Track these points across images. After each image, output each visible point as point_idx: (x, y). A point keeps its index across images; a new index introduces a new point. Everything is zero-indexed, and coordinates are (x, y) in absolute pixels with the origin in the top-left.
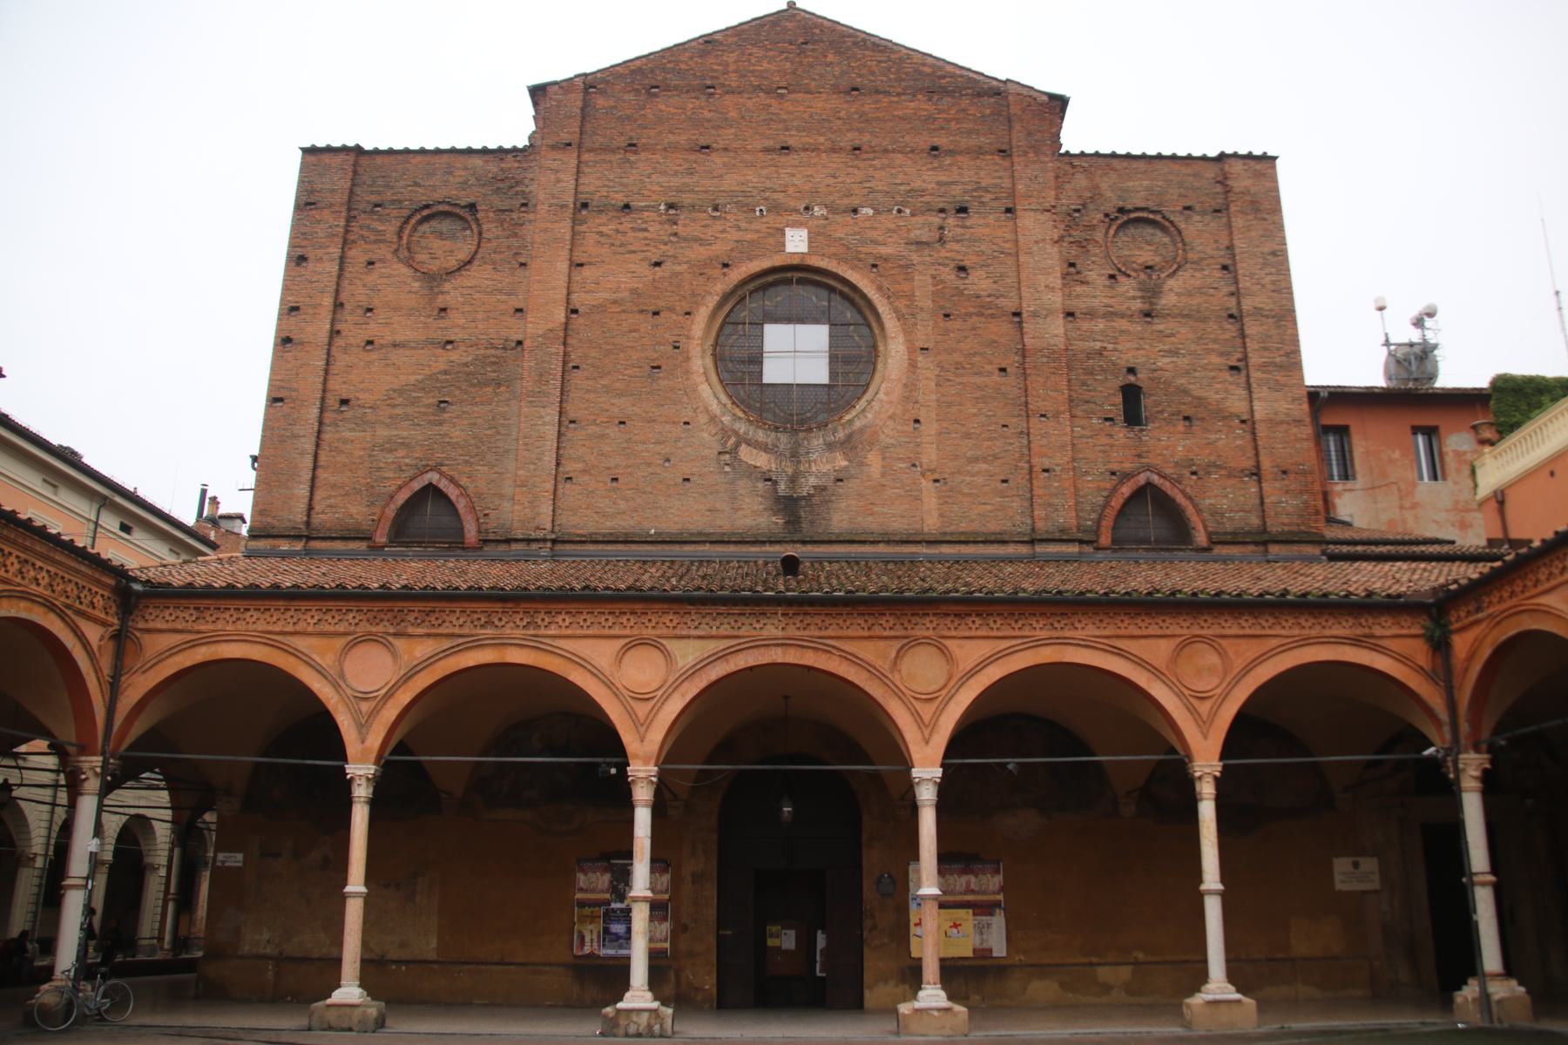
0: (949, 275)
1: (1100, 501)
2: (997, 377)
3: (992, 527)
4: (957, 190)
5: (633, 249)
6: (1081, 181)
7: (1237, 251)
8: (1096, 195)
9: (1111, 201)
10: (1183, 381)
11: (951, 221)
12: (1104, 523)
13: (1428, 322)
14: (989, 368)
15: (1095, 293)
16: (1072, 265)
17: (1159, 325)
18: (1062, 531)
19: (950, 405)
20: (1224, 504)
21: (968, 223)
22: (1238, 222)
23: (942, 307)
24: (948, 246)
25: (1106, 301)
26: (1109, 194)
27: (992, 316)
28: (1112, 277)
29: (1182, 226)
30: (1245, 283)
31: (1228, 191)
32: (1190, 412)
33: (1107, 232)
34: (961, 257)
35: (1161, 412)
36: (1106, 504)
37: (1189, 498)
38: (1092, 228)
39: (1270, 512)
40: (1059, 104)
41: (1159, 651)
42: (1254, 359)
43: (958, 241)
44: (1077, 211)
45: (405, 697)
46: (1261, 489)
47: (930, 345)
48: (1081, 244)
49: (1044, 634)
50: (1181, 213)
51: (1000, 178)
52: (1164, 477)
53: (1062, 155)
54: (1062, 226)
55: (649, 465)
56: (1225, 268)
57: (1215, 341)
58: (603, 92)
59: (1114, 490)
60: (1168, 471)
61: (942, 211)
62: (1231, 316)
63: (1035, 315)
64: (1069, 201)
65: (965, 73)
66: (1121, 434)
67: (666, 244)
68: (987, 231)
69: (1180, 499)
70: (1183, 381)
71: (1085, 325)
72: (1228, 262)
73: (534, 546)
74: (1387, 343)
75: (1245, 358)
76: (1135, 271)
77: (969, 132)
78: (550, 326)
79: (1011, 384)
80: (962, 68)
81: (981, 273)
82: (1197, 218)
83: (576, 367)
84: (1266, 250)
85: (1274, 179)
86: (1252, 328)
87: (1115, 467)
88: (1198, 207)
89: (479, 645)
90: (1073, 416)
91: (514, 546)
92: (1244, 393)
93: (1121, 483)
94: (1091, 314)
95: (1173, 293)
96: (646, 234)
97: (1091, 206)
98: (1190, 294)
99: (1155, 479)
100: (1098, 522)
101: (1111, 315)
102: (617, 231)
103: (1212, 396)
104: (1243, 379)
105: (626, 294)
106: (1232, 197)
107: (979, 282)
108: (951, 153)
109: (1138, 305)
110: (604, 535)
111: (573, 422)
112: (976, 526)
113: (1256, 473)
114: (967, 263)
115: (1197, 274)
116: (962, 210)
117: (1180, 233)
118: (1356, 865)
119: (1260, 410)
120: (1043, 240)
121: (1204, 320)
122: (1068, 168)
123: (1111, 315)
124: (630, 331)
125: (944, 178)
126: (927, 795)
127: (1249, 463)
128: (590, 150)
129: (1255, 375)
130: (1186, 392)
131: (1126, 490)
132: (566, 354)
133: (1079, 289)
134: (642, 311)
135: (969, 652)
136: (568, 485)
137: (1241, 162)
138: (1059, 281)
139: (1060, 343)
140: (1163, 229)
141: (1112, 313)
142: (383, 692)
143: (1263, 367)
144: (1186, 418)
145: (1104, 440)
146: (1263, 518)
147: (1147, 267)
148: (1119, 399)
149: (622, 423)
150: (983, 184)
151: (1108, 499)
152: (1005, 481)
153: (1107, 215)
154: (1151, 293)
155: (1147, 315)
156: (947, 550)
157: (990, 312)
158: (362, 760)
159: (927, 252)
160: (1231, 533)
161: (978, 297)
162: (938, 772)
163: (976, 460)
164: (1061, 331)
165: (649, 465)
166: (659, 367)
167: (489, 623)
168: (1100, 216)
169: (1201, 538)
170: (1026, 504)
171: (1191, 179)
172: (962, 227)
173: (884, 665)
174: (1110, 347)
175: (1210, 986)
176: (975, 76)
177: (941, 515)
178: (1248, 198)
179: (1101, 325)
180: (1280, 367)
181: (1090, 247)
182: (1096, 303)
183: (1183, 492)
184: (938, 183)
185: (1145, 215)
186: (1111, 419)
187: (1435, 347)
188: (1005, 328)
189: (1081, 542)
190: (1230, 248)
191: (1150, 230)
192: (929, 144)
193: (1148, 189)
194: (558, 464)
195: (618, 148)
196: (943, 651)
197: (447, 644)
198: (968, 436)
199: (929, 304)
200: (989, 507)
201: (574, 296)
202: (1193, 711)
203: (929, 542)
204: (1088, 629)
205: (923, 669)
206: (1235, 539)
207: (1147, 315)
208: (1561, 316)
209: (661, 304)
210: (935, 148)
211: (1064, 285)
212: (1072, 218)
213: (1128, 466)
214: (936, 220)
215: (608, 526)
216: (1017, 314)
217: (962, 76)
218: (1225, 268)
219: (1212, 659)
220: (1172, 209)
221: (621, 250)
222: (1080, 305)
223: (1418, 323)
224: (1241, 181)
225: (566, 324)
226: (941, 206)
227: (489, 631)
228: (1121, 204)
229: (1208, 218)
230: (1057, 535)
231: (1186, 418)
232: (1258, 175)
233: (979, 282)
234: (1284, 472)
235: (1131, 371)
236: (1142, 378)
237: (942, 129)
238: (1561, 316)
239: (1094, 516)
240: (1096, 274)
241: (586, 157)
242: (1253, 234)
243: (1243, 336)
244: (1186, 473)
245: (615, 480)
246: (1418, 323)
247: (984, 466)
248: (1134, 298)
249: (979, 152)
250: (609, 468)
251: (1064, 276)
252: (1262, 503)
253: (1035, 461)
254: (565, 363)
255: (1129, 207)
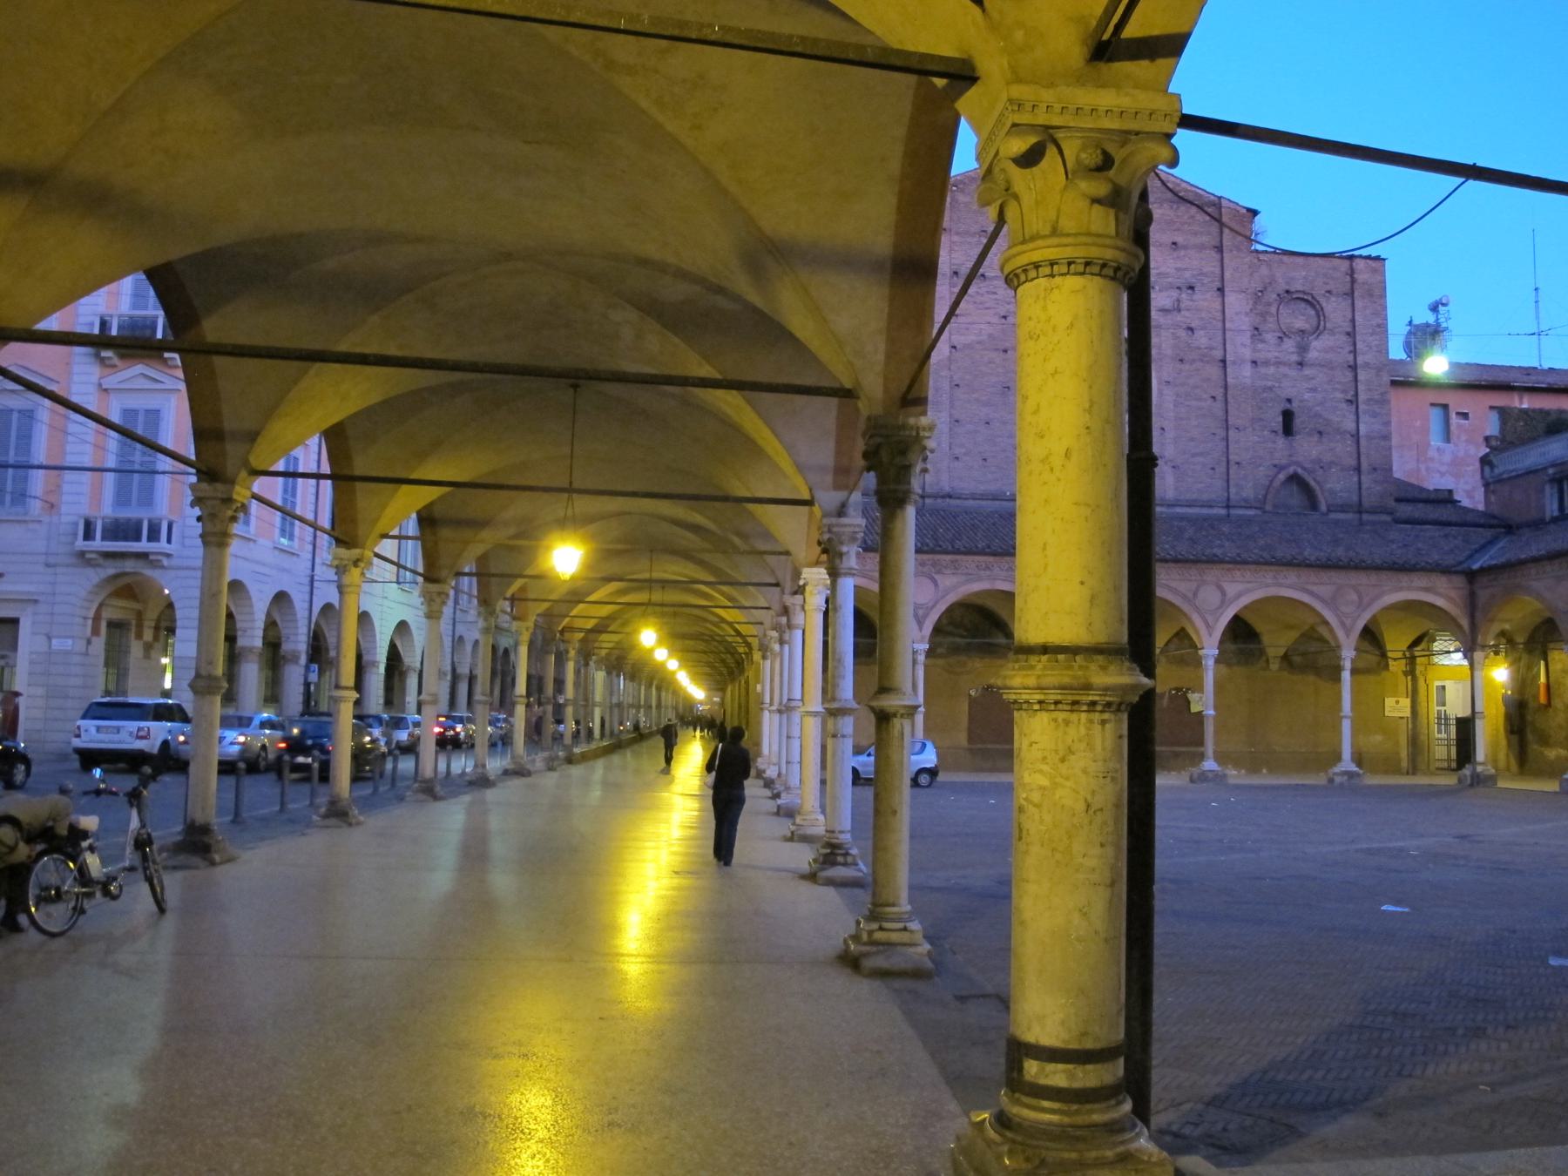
0: (1182, 333)
1: (1267, 483)
2: (1210, 401)
3: (1205, 497)
4: (1187, 274)
5: (987, 305)
6: (1264, 271)
7: (1357, 324)
8: (1272, 281)
9: (1282, 286)
10: (1318, 408)
11: (1184, 296)
12: (1269, 497)
13: (1441, 308)
14: (1205, 396)
15: (1269, 350)
16: (1256, 329)
17: (1307, 371)
18: (1246, 500)
19: (1182, 419)
20: (1338, 487)
21: (1195, 297)
22: (1359, 304)
23: (1178, 355)
24: (1183, 313)
25: (1276, 354)
26: (1280, 280)
27: (1208, 362)
28: (1280, 338)
29: (1324, 305)
30: (1360, 345)
31: (1353, 281)
32: (1321, 429)
33: (1278, 309)
34: (1189, 321)
35: (1305, 428)
36: (1269, 487)
37: (1318, 483)
38: (1269, 304)
39: (1364, 493)
40: (1254, 213)
41: (1326, 590)
42: (1362, 397)
43: (1188, 310)
44: (1261, 291)
45: (942, 607)
46: (1360, 479)
47: (1170, 379)
48: (1263, 315)
49: (1270, 581)
50: (1324, 296)
51: (1214, 267)
52: (1304, 469)
53: (1252, 252)
54: (1251, 302)
55: (1004, 451)
56: (1348, 334)
57: (1339, 383)
58: (962, 191)
59: (1276, 476)
60: (1306, 465)
61: (1179, 288)
62: (1350, 366)
63: (1234, 363)
64: (1256, 285)
65: (1194, 189)
66: (1281, 441)
67: (1009, 304)
68: (1206, 304)
69: (1312, 483)
70: (1318, 408)
71: (1263, 370)
72: (1349, 330)
73: (939, 501)
74: (1410, 323)
75: (1356, 395)
76: (1293, 333)
77: (1195, 234)
78: (941, 357)
79: (1219, 405)
80: (1192, 185)
81: (1202, 332)
82: (1333, 299)
83: (957, 385)
84: (1374, 323)
85: (1383, 273)
86: (1362, 376)
87: (1276, 462)
88: (1334, 292)
89: (980, 579)
90: (1254, 429)
91: (928, 501)
92: (1353, 417)
93: (1279, 473)
94: (1266, 363)
95: (1318, 348)
96: (996, 296)
97: (1269, 289)
98: (1326, 352)
99: (1300, 471)
100: (1265, 497)
101: (1278, 363)
102: (978, 293)
103: (1335, 419)
104: (1354, 410)
105: (985, 337)
106: (1356, 286)
107: (1201, 339)
108: (1185, 247)
109: (1295, 358)
110: (982, 495)
111: (957, 421)
112: (1194, 496)
113: (1358, 469)
114: (1193, 325)
115: (1332, 338)
116: (1192, 288)
117: (1322, 309)
118: (1397, 702)
119: (1363, 429)
120: (1240, 313)
121: (1332, 369)
122: (1256, 261)
123: (1278, 363)
124: (990, 363)
125: (1179, 265)
126: (1210, 663)
127: (1353, 463)
128: (957, 234)
129: (1361, 407)
130: (1320, 416)
131: (1282, 476)
132: (951, 377)
133: (1260, 346)
134: (997, 350)
135: (1231, 589)
136: (956, 463)
137: (1364, 261)
138: (1249, 341)
139: (1248, 381)
140: (1313, 306)
141: (1280, 363)
142: (930, 605)
143: (1368, 401)
144: (1320, 433)
145: (1270, 445)
146: (1360, 496)
147: (1302, 331)
148: (1280, 419)
149: (988, 423)
150: (1205, 270)
151: (1271, 482)
152: (1213, 469)
153: (1279, 295)
154: (1303, 349)
155: (1301, 364)
156: (1179, 510)
157: (1206, 359)
158: (922, 641)
159: (1169, 317)
160: (1342, 506)
161: (1199, 348)
162: (1217, 652)
163: (1194, 455)
164: (1248, 374)
165: (1004, 451)
166: (1008, 388)
167: (987, 568)
168: (1275, 296)
169: (1323, 508)
170: (1225, 485)
171: (1331, 272)
172: (1192, 300)
173: (1190, 595)
174: (1277, 385)
175: (1343, 764)
176: (1202, 193)
177: (1176, 489)
178: (1366, 287)
179: (1272, 370)
180: (1377, 402)
181: (1268, 317)
182: (1270, 355)
183: (1315, 480)
184: (1176, 269)
185: (1301, 296)
186: (1275, 432)
187: (1446, 329)
188: (1214, 372)
189: (1256, 508)
190: (1353, 321)
191: (1303, 305)
192: (1171, 241)
193: (1305, 278)
194: (950, 449)
195: (975, 233)
196: (1220, 588)
197: (964, 578)
198: (1192, 440)
199: (1169, 352)
200: (1203, 485)
201: (953, 337)
202: (1343, 624)
203: (1169, 506)
204: (1292, 576)
205: (1209, 596)
206: (1343, 508)
207: (1301, 364)
208: (1537, 308)
209: (1007, 345)
210: (1174, 243)
211: (1252, 343)
212: (1258, 296)
213: (1284, 462)
214: (1175, 294)
215: (982, 488)
216: (1224, 361)
217: (1192, 191)
218: (1348, 334)
219: (1354, 597)
220: (1319, 292)
221: (981, 306)
222: (1260, 356)
223: (1434, 308)
224: (1363, 272)
225: (949, 359)
226: (1178, 285)
227: (988, 573)
228: (1287, 288)
229: (1340, 299)
230: (1243, 504)
231: (1320, 433)
232: (1375, 271)
233: (1201, 339)
234: (1375, 469)
235: (1289, 401)
236: (1295, 406)
237: (1178, 230)
238: (1537, 308)
239: (1263, 492)
240: (1270, 337)
241: (955, 238)
242: (1368, 312)
243: (1356, 380)
244: (1317, 467)
245: (985, 460)
246: (1434, 308)
247: (1201, 459)
248: (1293, 353)
249: (1201, 247)
250: (980, 453)
251: (1253, 336)
252: (1360, 488)
253: (1231, 457)
254: (950, 382)
255: (1293, 290)
